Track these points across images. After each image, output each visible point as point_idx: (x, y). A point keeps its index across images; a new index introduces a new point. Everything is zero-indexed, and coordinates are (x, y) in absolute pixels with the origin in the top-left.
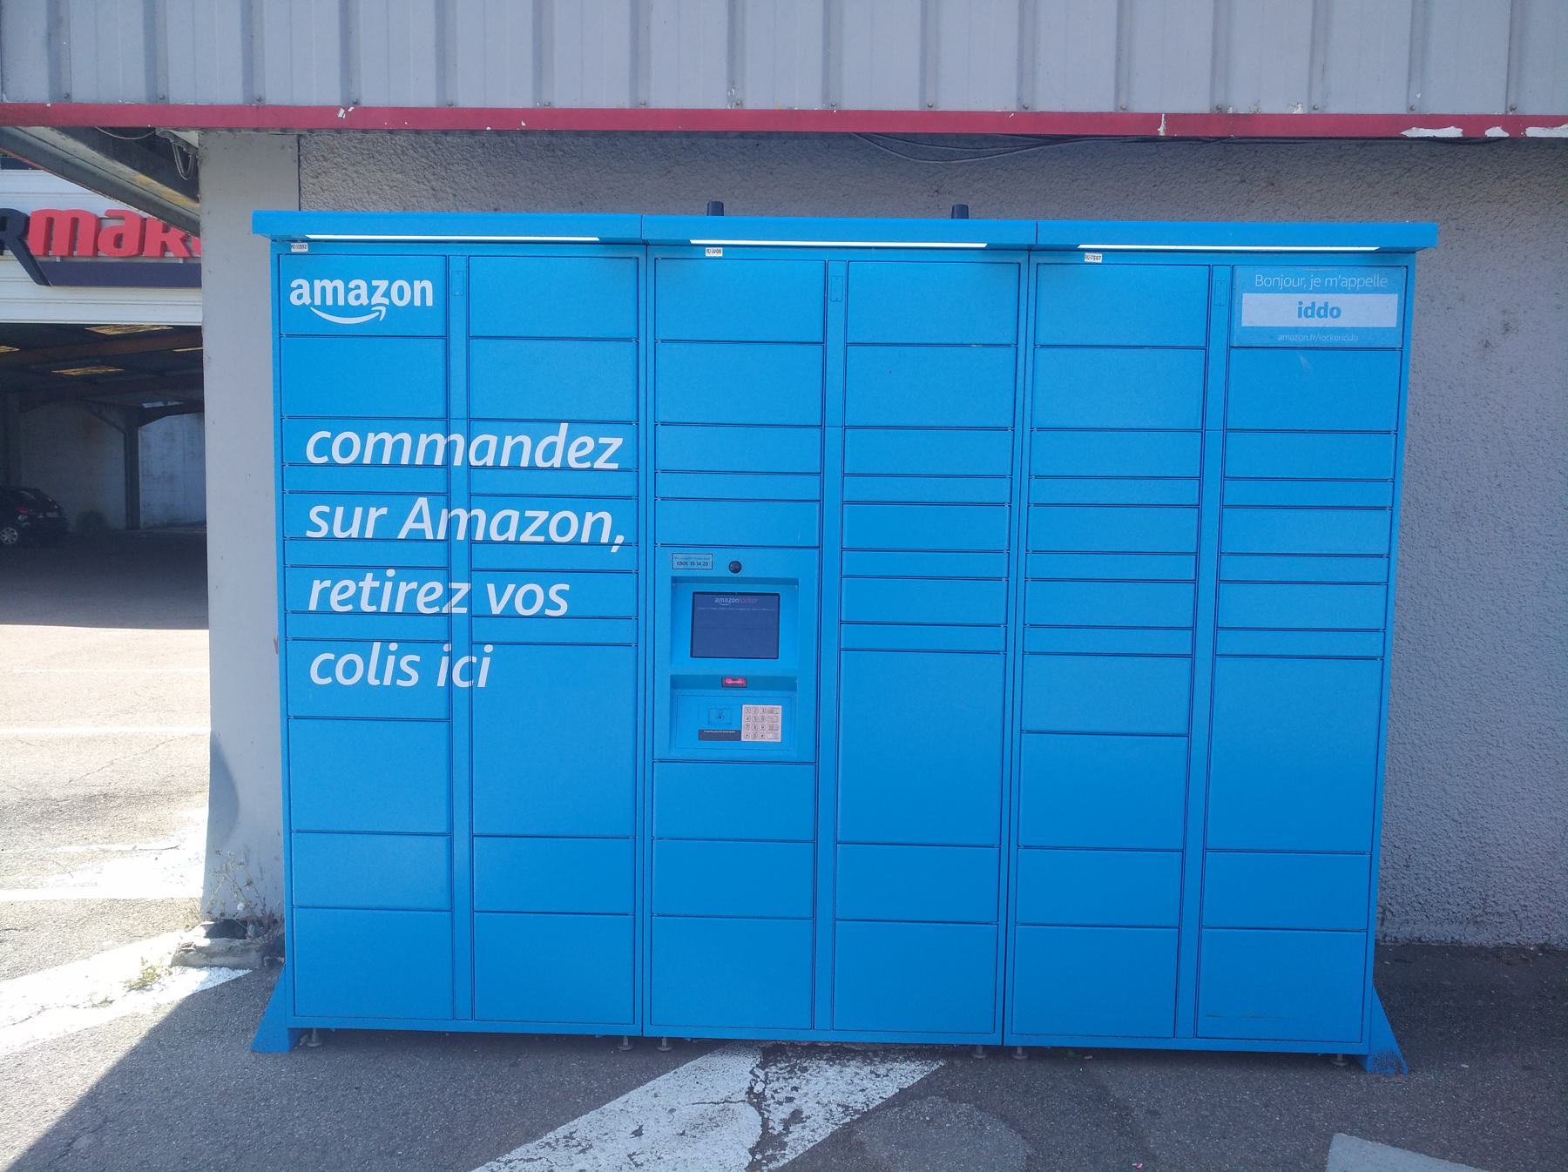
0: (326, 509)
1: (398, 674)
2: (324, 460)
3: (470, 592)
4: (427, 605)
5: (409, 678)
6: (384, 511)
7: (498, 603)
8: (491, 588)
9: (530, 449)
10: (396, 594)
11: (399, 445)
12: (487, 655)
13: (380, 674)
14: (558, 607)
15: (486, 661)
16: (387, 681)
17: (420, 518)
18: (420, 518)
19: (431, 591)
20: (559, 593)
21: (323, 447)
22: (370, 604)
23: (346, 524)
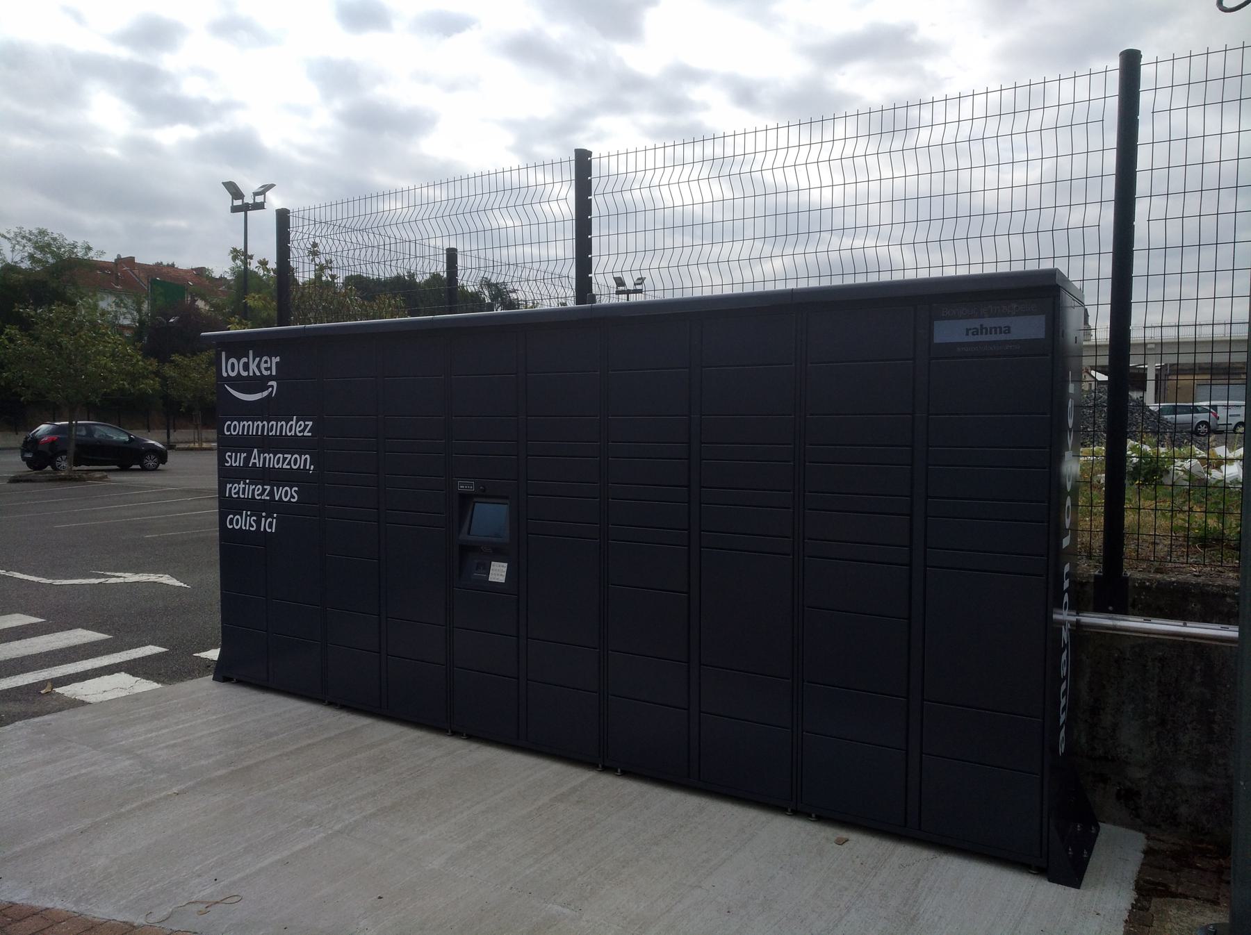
4: (258, 495)
8: (275, 488)
11: (249, 425)
12: (274, 518)
13: (245, 526)
15: (275, 520)
17: (257, 460)
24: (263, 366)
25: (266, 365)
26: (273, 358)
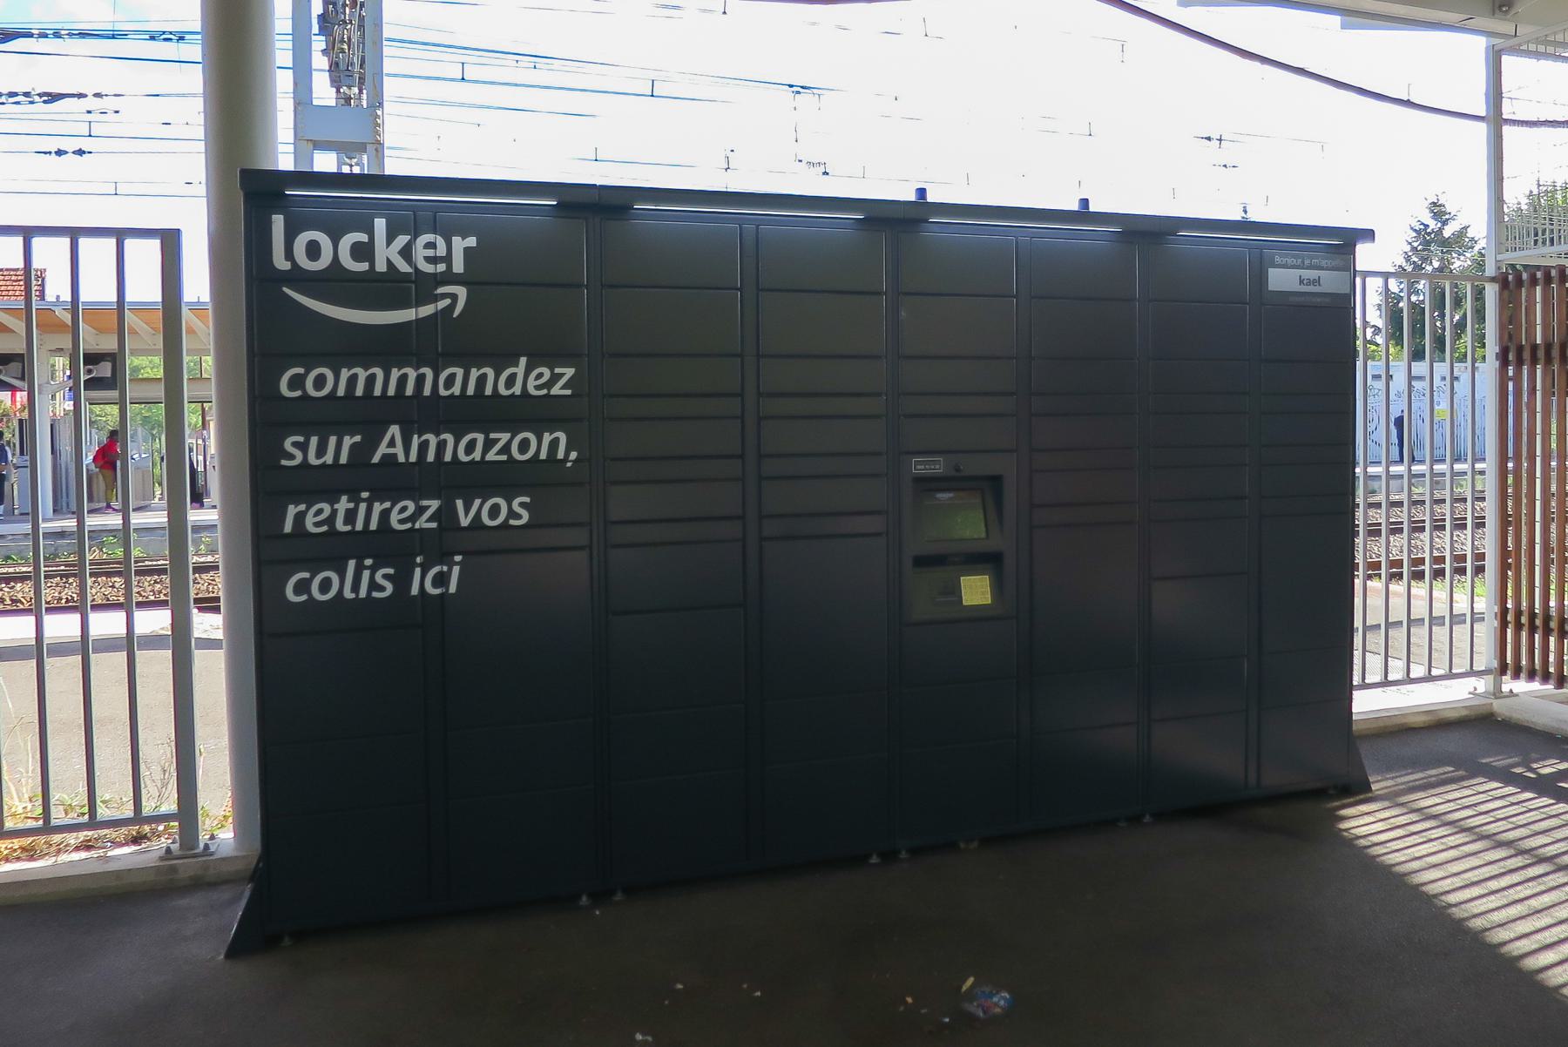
0: (301, 439)
1: (374, 586)
2: (298, 393)
3: (439, 510)
4: (401, 522)
5: (382, 589)
6: (358, 438)
7: (466, 514)
8: (459, 503)
9: (495, 382)
10: (369, 514)
11: (371, 380)
12: (457, 564)
13: (356, 588)
14: (519, 517)
15: (456, 570)
16: (363, 593)
17: (392, 444)
18: (392, 444)
19: (404, 509)
20: (522, 505)
21: (297, 382)
22: (346, 523)
23: (321, 451)
24: (420, 253)
25: (430, 253)
26: (456, 240)
